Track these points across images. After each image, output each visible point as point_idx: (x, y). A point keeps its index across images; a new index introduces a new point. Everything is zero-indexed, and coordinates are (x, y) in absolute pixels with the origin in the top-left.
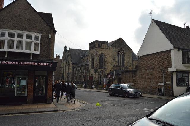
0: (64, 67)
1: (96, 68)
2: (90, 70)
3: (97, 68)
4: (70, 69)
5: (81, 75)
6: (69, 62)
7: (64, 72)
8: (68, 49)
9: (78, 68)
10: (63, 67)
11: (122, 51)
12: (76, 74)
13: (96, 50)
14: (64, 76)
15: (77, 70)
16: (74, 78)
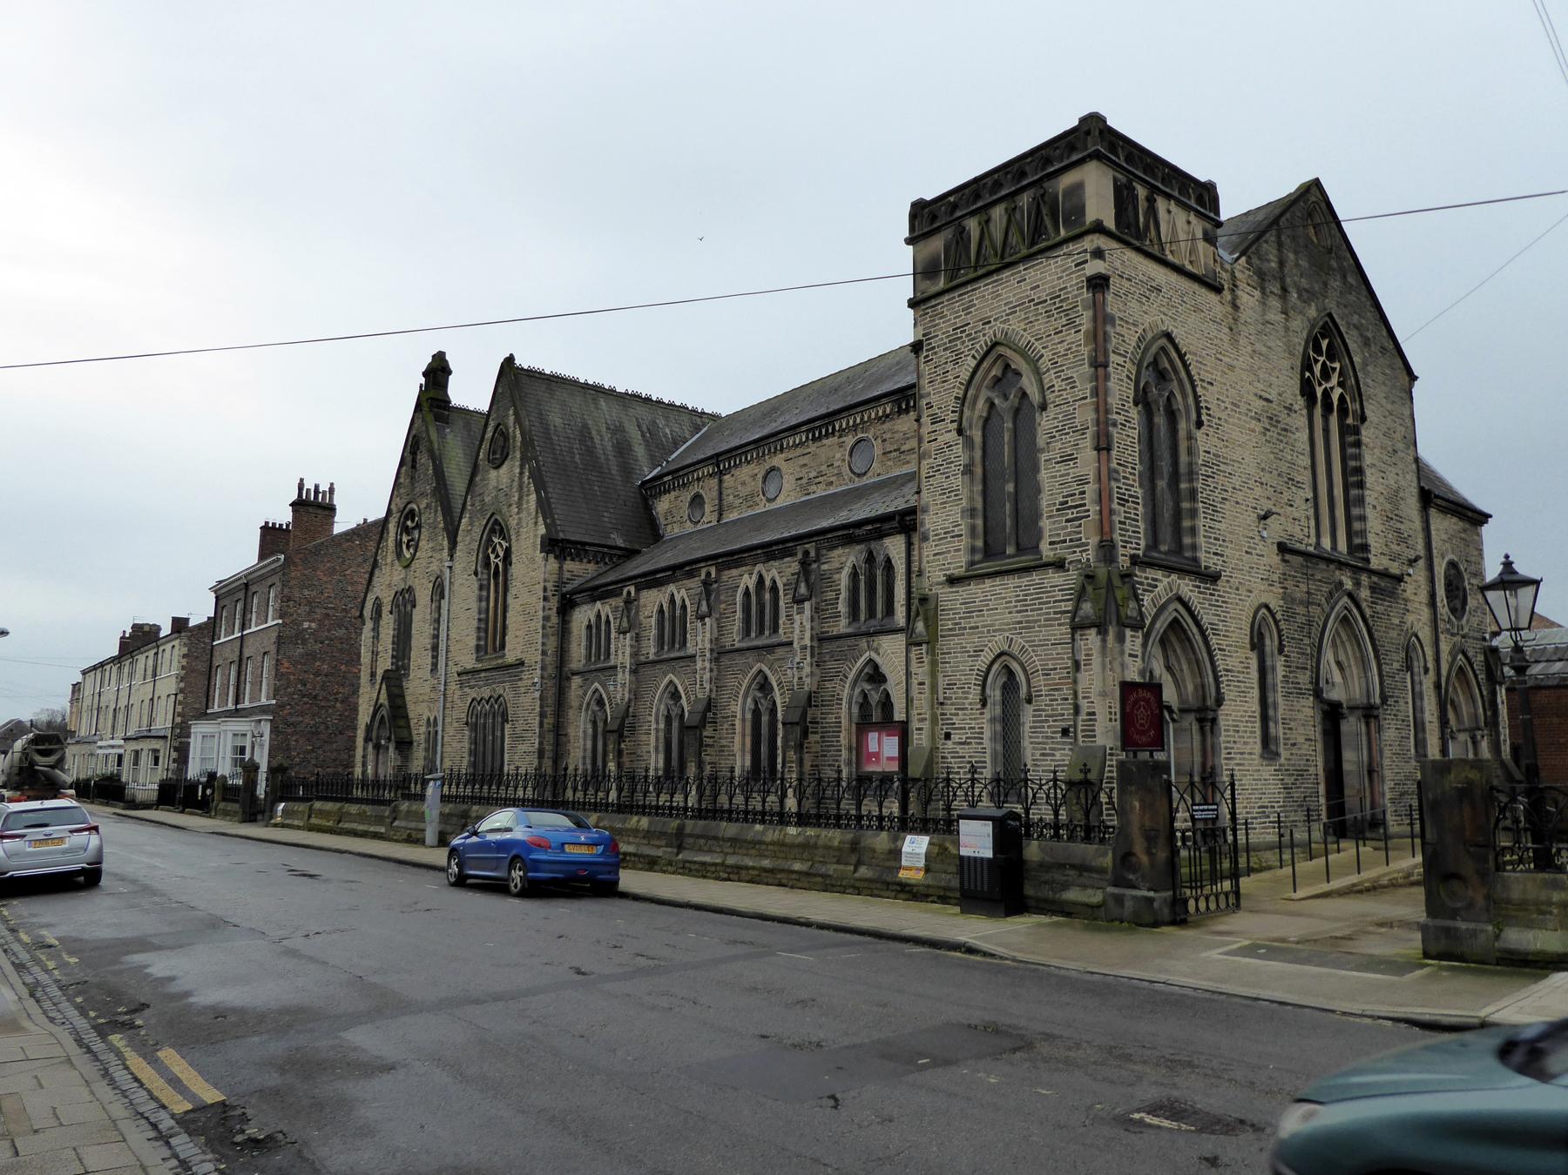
0: (423, 596)
1: (1107, 549)
2: (952, 600)
3: (1123, 562)
4: (513, 618)
5: (718, 682)
6: (497, 528)
7: (419, 657)
8: (472, 390)
9: (652, 600)
10: (405, 600)
11: (1331, 356)
12: (623, 677)
13: (1095, 267)
14: (419, 710)
15: (632, 626)
16: (579, 729)
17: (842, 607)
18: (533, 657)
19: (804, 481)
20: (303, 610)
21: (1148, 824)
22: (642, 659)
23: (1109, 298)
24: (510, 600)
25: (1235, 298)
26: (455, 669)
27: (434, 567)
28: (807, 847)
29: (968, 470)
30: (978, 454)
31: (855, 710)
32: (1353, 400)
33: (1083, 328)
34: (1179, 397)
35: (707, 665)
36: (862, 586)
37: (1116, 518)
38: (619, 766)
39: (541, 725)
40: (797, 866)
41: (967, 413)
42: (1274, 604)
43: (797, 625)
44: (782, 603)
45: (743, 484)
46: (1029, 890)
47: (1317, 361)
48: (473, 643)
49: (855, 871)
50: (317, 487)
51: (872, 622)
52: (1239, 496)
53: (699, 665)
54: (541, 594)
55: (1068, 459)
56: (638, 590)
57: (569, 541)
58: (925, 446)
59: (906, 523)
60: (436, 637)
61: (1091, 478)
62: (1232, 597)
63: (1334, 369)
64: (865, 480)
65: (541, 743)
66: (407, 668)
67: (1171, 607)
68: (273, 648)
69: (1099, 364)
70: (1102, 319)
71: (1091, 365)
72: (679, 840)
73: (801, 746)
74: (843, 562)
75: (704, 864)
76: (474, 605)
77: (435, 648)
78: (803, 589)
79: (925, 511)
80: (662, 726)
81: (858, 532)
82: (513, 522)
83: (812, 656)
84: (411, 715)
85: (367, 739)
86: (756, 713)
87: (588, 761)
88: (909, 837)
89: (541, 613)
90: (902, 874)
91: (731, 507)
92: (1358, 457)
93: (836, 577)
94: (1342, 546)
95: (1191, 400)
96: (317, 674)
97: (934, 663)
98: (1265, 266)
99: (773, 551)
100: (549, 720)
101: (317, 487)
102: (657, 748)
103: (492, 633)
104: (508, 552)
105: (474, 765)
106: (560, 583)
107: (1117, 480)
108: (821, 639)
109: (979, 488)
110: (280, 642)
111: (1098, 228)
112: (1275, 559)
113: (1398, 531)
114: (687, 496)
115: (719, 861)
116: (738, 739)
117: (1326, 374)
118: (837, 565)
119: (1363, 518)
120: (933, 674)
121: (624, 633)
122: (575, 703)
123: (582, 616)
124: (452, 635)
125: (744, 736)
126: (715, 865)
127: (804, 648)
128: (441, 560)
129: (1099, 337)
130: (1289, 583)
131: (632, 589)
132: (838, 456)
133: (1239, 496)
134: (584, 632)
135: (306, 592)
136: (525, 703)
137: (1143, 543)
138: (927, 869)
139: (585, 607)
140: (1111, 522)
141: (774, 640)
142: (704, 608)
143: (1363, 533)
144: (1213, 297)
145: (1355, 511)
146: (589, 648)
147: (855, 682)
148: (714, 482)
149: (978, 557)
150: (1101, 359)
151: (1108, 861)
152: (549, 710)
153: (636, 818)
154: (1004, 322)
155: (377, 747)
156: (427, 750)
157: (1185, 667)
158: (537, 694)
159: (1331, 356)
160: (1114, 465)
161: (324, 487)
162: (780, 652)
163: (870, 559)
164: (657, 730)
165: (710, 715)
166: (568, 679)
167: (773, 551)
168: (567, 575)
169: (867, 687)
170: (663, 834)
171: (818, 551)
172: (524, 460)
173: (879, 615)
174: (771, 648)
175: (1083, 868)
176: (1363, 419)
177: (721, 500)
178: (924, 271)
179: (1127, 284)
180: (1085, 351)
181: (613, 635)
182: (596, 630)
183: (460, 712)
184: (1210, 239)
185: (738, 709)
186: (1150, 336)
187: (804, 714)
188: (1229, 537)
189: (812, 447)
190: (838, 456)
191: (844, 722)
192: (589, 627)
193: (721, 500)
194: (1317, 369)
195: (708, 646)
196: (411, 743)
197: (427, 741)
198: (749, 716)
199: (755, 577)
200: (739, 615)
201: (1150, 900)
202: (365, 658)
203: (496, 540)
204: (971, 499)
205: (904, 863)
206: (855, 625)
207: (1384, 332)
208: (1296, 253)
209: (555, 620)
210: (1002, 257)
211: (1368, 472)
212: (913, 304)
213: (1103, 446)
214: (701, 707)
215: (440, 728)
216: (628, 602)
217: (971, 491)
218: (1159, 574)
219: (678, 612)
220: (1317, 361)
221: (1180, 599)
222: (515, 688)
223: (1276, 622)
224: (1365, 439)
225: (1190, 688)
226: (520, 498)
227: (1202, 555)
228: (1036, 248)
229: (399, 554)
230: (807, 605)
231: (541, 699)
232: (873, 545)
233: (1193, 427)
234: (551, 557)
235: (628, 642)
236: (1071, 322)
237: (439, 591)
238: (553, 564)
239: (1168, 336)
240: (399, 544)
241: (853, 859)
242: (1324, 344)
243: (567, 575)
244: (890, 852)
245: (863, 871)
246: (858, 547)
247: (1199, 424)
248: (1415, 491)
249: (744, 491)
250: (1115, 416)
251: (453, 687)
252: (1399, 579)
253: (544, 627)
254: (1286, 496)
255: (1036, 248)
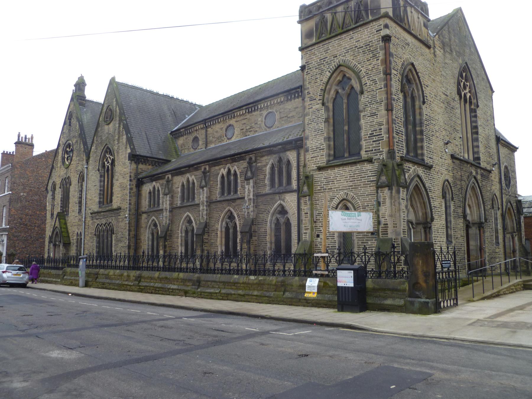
0: (74, 180)
1: (391, 153)
2: (320, 177)
4: (116, 189)
5: (209, 215)
6: (108, 150)
7: (73, 207)
8: (96, 93)
9: (179, 181)
10: (66, 183)
11: (466, 80)
12: (166, 214)
13: (386, 32)
14: (73, 230)
15: (170, 192)
16: (146, 237)
17: (267, 182)
18: (125, 205)
19: (244, 130)
20: (21, 187)
21: (425, 269)
22: (175, 206)
23: (391, 46)
24: (114, 181)
25: (435, 52)
26: (89, 211)
27: (80, 168)
28: (260, 284)
29: (327, 121)
30: (331, 114)
31: (273, 226)
32: (474, 98)
33: (380, 58)
34: (416, 91)
35: (205, 208)
36: (276, 172)
37: (395, 140)
38: (165, 252)
39: (129, 235)
40: (256, 293)
41: (326, 96)
42: (450, 180)
43: (246, 190)
44: (239, 181)
45: (217, 132)
46: (369, 301)
47: (462, 81)
48: (97, 200)
49: (284, 294)
50: (26, 136)
51: (281, 188)
52: (438, 134)
53: (201, 208)
54: (129, 179)
55: (373, 115)
56: (173, 176)
57: (141, 156)
58: (307, 110)
59: (298, 144)
60: (81, 198)
61: (384, 123)
62: (436, 176)
63: (467, 85)
64: (272, 130)
65: (129, 243)
66: (67, 211)
67: (415, 179)
68: (8, 204)
69: (387, 73)
70: (388, 55)
71: (384, 74)
72: (198, 283)
73: (250, 241)
74: (267, 163)
75: (211, 293)
76: (98, 184)
77: (80, 202)
78: (249, 174)
79: (307, 138)
80: (184, 235)
81: (274, 149)
82: (116, 148)
83: (254, 203)
84: (70, 231)
85: (50, 242)
86: (227, 229)
87: (150, 250)
88: (309, 279)
89: (129, 187)
90: (306, 295)
91: (211, 142)
92: (476, 122)
93: (264, 169)
94: (471, 158)
95: (421, 92)
96: (27, 215)
97: (312, 204)
98: (444, 40)
99: (235, 158)
100: (133, 233)
101: (26, 136)
102: (181, 244)
103: (106, 195)
104: (113, 161)
105: (98, 252)
106: (137, 174)
107: (395, 124)
108: (257, 196)
109: (332, 128)
110: (10, 201)
111: (386, 15)
112: (449, 161)
113: (489, 153)
114: (191, 137)
115: (217, 291)
116: (219, 239)
117: (465, 88)
118: (264, 163)
119: (478, 147)
120: (312, 210)
121: (166, 195)
122: (144, 225)
123: (147, 188)
124: (88, 197)
125: (221, 238)
126: (216, 293)
127: (250, 199)
128: (83, 165)
129: (387, 62)
130: (455, 172)
131: (170, 176)
132: (259, 119)
133: (438, 134)
134: (147, 195)
135: (22, 180)
136: (122, 225)
137: (405, 151)
138: (319, 292)
139: (148, 184)
140: (393, 142)
141: (235, 196)
142: (203, 183)
143: (478, 153)
144: (427, 50)
145: (475, 144)
146: (150, 202)
147: (273, 214)
148: (203, 131)
149: (331, 158)
150: (388, 71)
151: (406, 286)
152: (132, 229)
153: (177, 274)
154: (343, 56)
155: (55, 245)
156: (77, 246)
157: (419, 205)
158: (127, 222)
159: (466, 80)
160: (394, 117)
161: (29, 136)
162: (238, 202)
163: (280, 160)
164: (181, 236)
165: (206, 229)
166: (141, 215)
167: (235, 158)
168: (140, 171)
169: (279, 216)
170: (190, 280)
171: (256, 157)
172: (120, 120)
173: (284, 185)
174: (234, 200)
175: (394, 290)
176: (478, 106)
177: (206, 139)
178: (307, 35)
179: (397, 41)
180: (381, 68)
181: (161, 196)
182: (153, 194)
183: (92, 229)
184: (426, 26)
185: (219, 227)
186: (406, 63)
187: (250, 228)
188: (435, 151)
189: (248, 116)
190: (259, 119)
191: (268, 231)
192: (150, 193)
193: (206, 139)
194: (462, 84)
195: (205, 199)
196: (70, 243)
197: (77, 242)
198: (224, 230)
199: (226, 170)
200: (219, 186)
201: (428, 303)
202: (49, 208)
203: (108, 156)
204: (328, 133)
205: (307, 290)
206: (273, 189)
207: (483, 73)
208: (454, 36)
209: (135, 190)
210: (342, 29)
211: (479, 128)
212: (301, 49)
213: (389, 109)
214: (203, 226)
215: (83, 237)
216: (168, 181)
217: (328, 130)
218: (410, 165)
219: (191, 186)
220: (462, 81)
221: (419, 176)
222: (117, 220)
223: (451, 187)
224: (478, 115)
225: (420, 214)
226: (119, 137)
227: (425, 158)
228: (358, 24)
229: (63, 162)
230: (251, 181)
231: (129, 223)
232: (282, 155)
233: (421, 104)
234: (133, 162)
235: (168, 198)
236: (374, 56)
237: (81, 178)
238: (134, 166)
239: (412, 64)
240: (63, 158)
241: (283, 289)
242: (464, 74)
243: (140, 171)
244: (300, 286)
245: (287, 294)
246: (274, 156)
247: (424, 103)
248: (494, 137)
249: (217, 135)
250: (394, 96)
251: (88, 219)
252: (490, 172)
253: (130, 193)
254: (453, 135)
255: (358, 24)
